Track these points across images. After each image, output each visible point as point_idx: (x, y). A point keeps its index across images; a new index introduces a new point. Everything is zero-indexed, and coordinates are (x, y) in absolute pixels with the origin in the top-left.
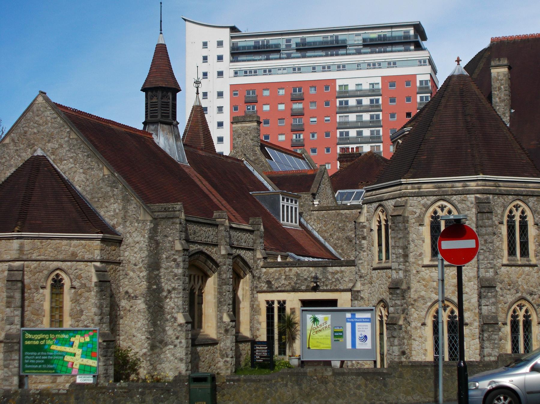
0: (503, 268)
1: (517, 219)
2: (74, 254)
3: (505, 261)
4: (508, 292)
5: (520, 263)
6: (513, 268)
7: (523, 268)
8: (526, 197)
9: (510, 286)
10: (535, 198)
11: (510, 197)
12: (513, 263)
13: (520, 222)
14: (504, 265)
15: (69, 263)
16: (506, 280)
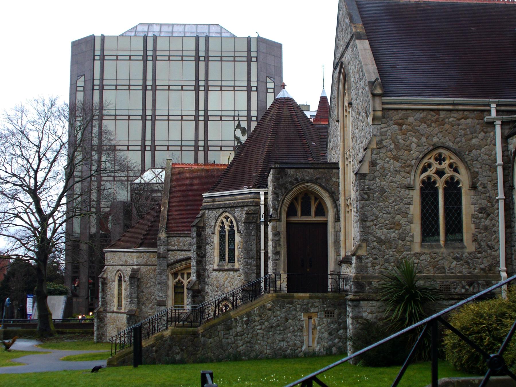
0: (214, 273)
1: (227, 229)
2: (126, 261)
3: (216, 267)
4: (216, 293)
5: (226, 268)
6: (221, 272)
7: (228, 272)
8: (232, 209)
9: (218, 288)
10: (240, 209)
11: (221, 210)
12: (221, 268)
13: (229, 231)
14: (214, 270)
15: (124, 267)
16: (215, 282)
